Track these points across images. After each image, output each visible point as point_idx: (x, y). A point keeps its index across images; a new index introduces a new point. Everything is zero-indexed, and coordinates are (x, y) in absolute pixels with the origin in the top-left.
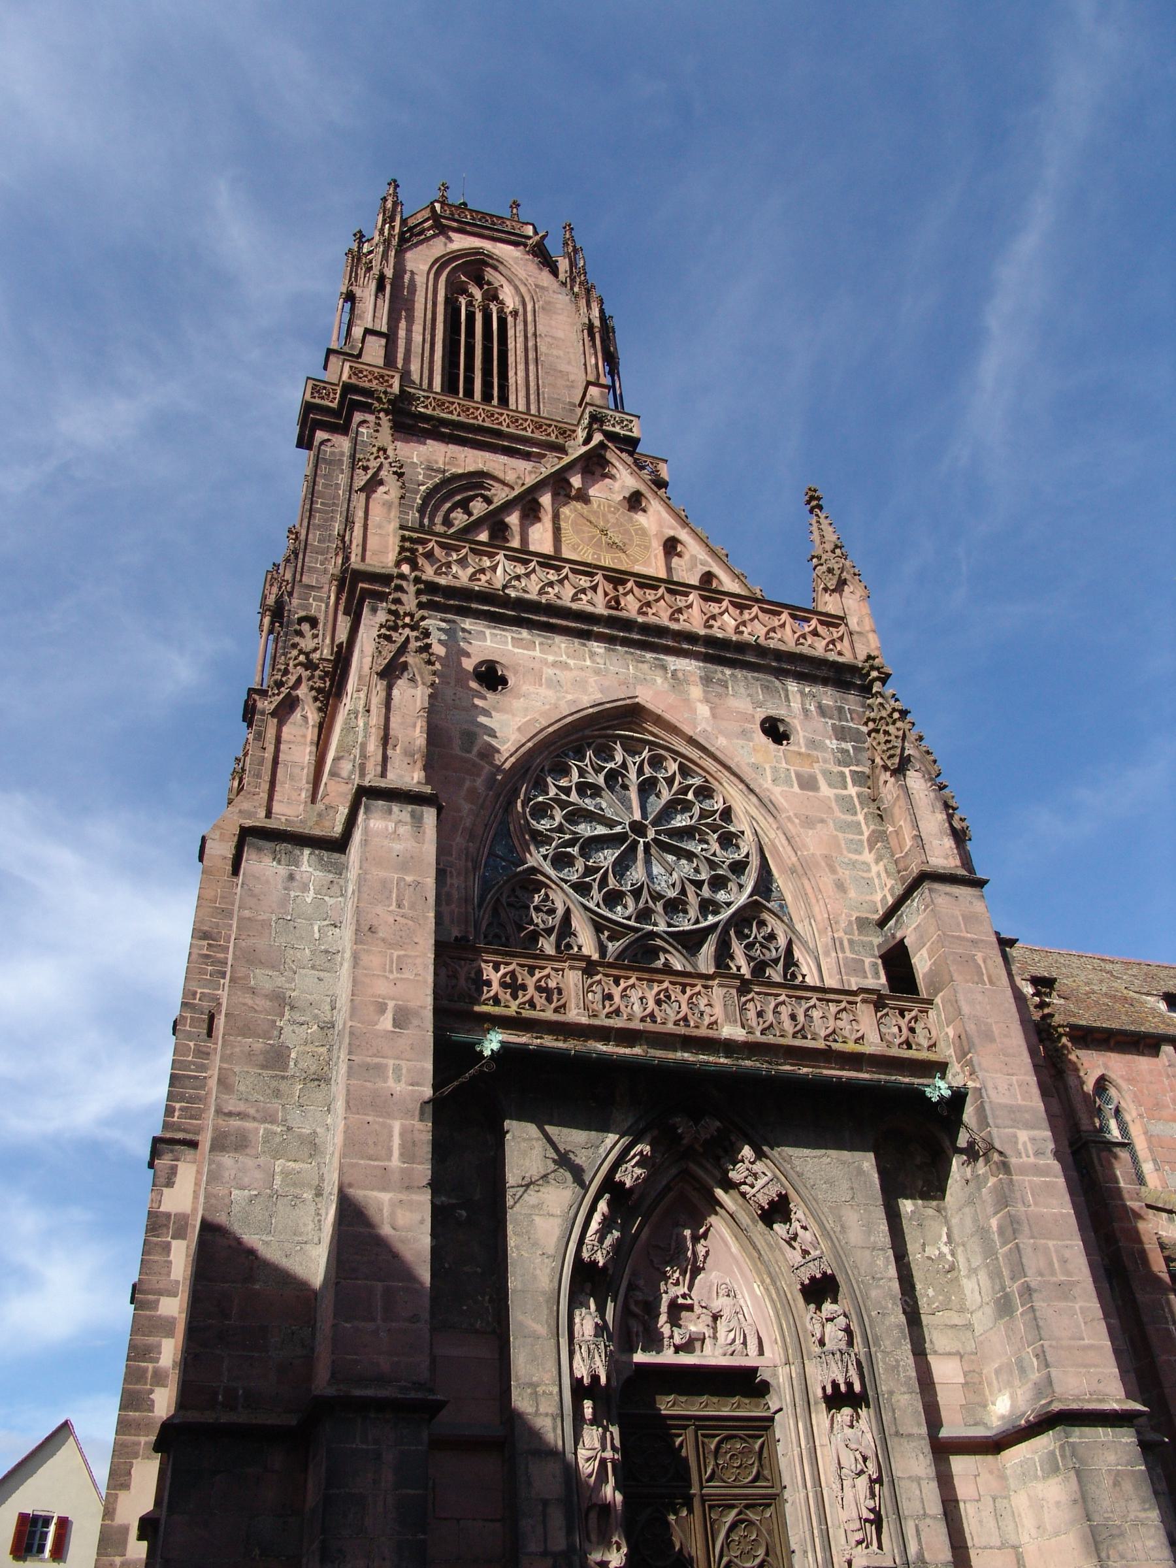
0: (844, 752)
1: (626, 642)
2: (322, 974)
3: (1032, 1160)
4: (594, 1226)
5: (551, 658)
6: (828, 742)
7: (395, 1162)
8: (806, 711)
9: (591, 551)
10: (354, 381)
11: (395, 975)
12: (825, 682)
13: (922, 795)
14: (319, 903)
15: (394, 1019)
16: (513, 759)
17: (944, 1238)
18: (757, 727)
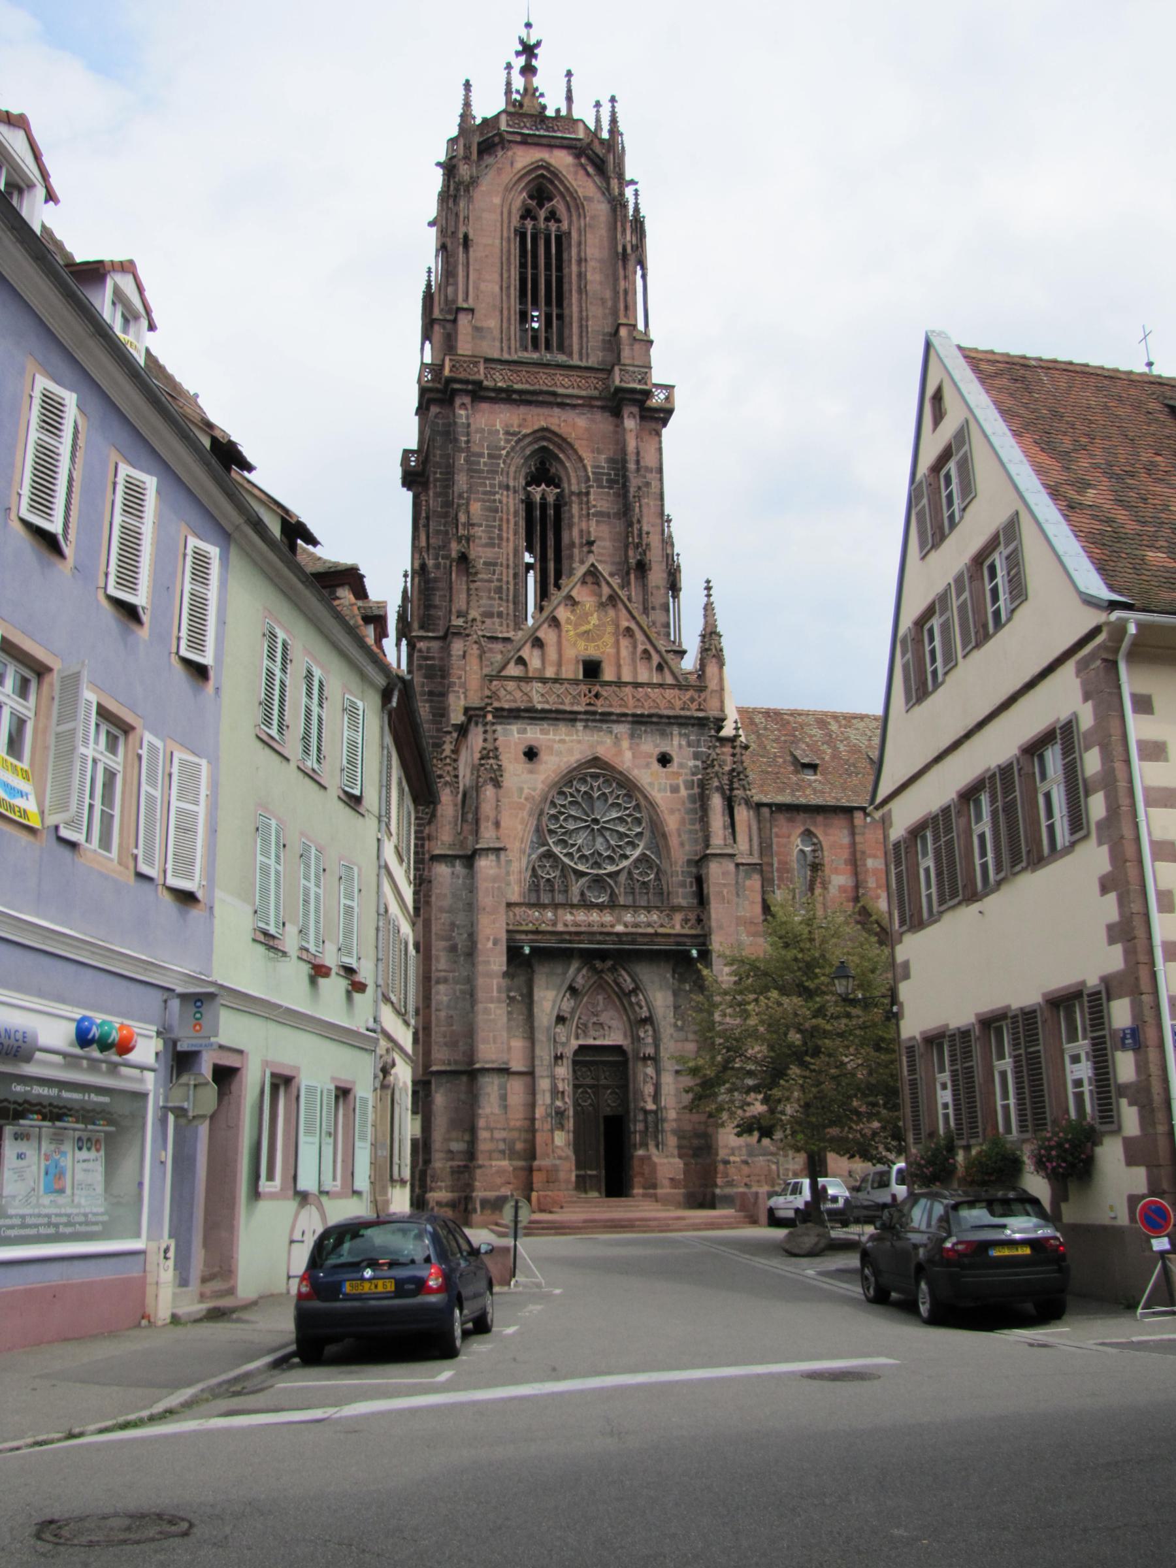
1: (594, 721)
5: (557, 738)
7: (495, 994)
8: (680, 746)
10: (453, 375)
12: (693, 725)
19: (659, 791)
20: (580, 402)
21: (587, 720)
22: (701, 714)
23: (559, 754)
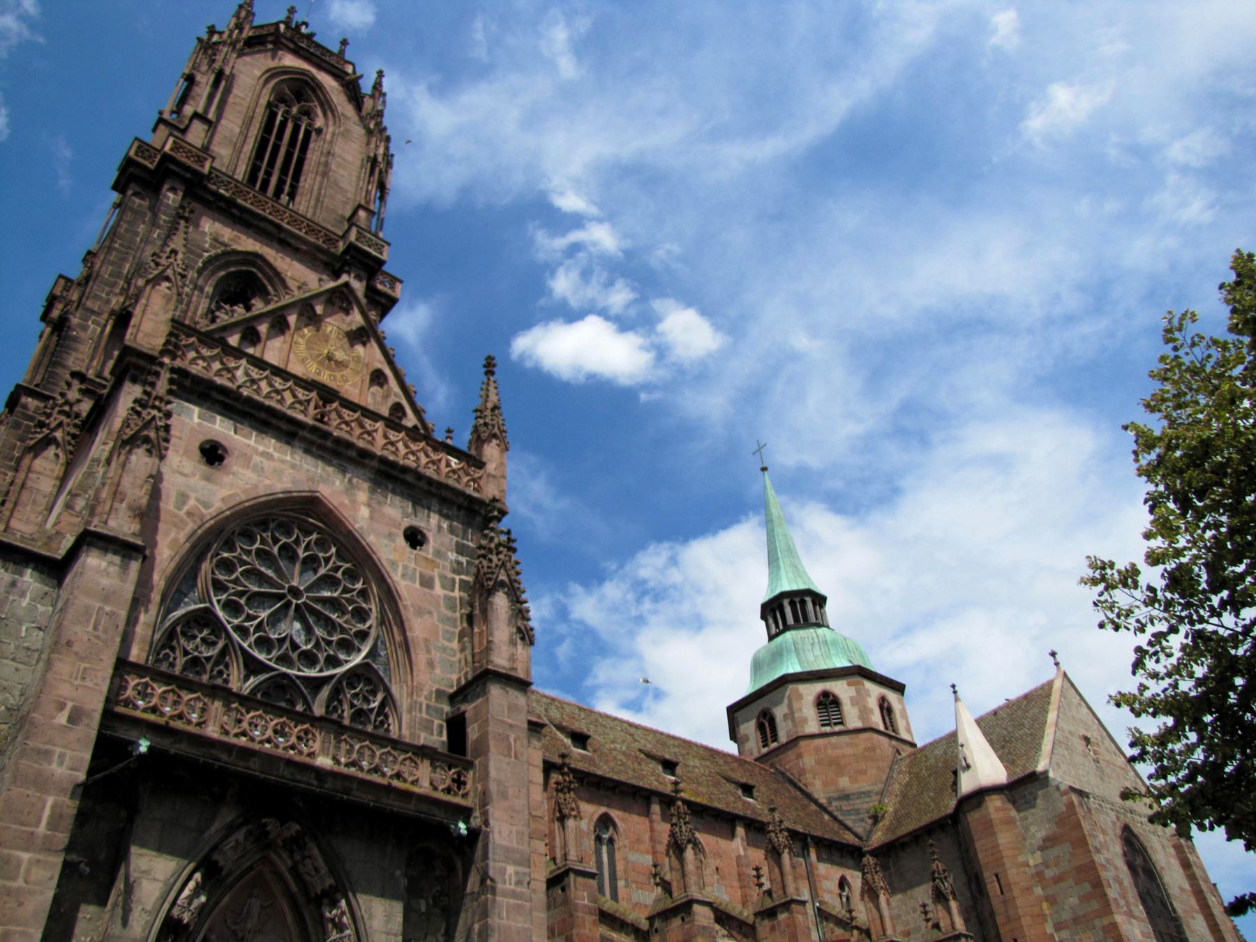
0: (459, 563)
1: (321, 447)
2: (20, 666)
3: (513, 887)
4: (186, 892)
6: (449, 554)
8: (440, 527)
9: (315, 366)
10: (172, 153)
11: (78, 682)
12: (460, 507)
13: (503, 611)
14: (31, 608)
15: (69, 717)
16: (212, 522)
17: (443, 931)
18: (401, 533)
19: (403, 576)
20: (304, 247)
21: (311, 443)
22: (475, 495)
23: (259, 470)
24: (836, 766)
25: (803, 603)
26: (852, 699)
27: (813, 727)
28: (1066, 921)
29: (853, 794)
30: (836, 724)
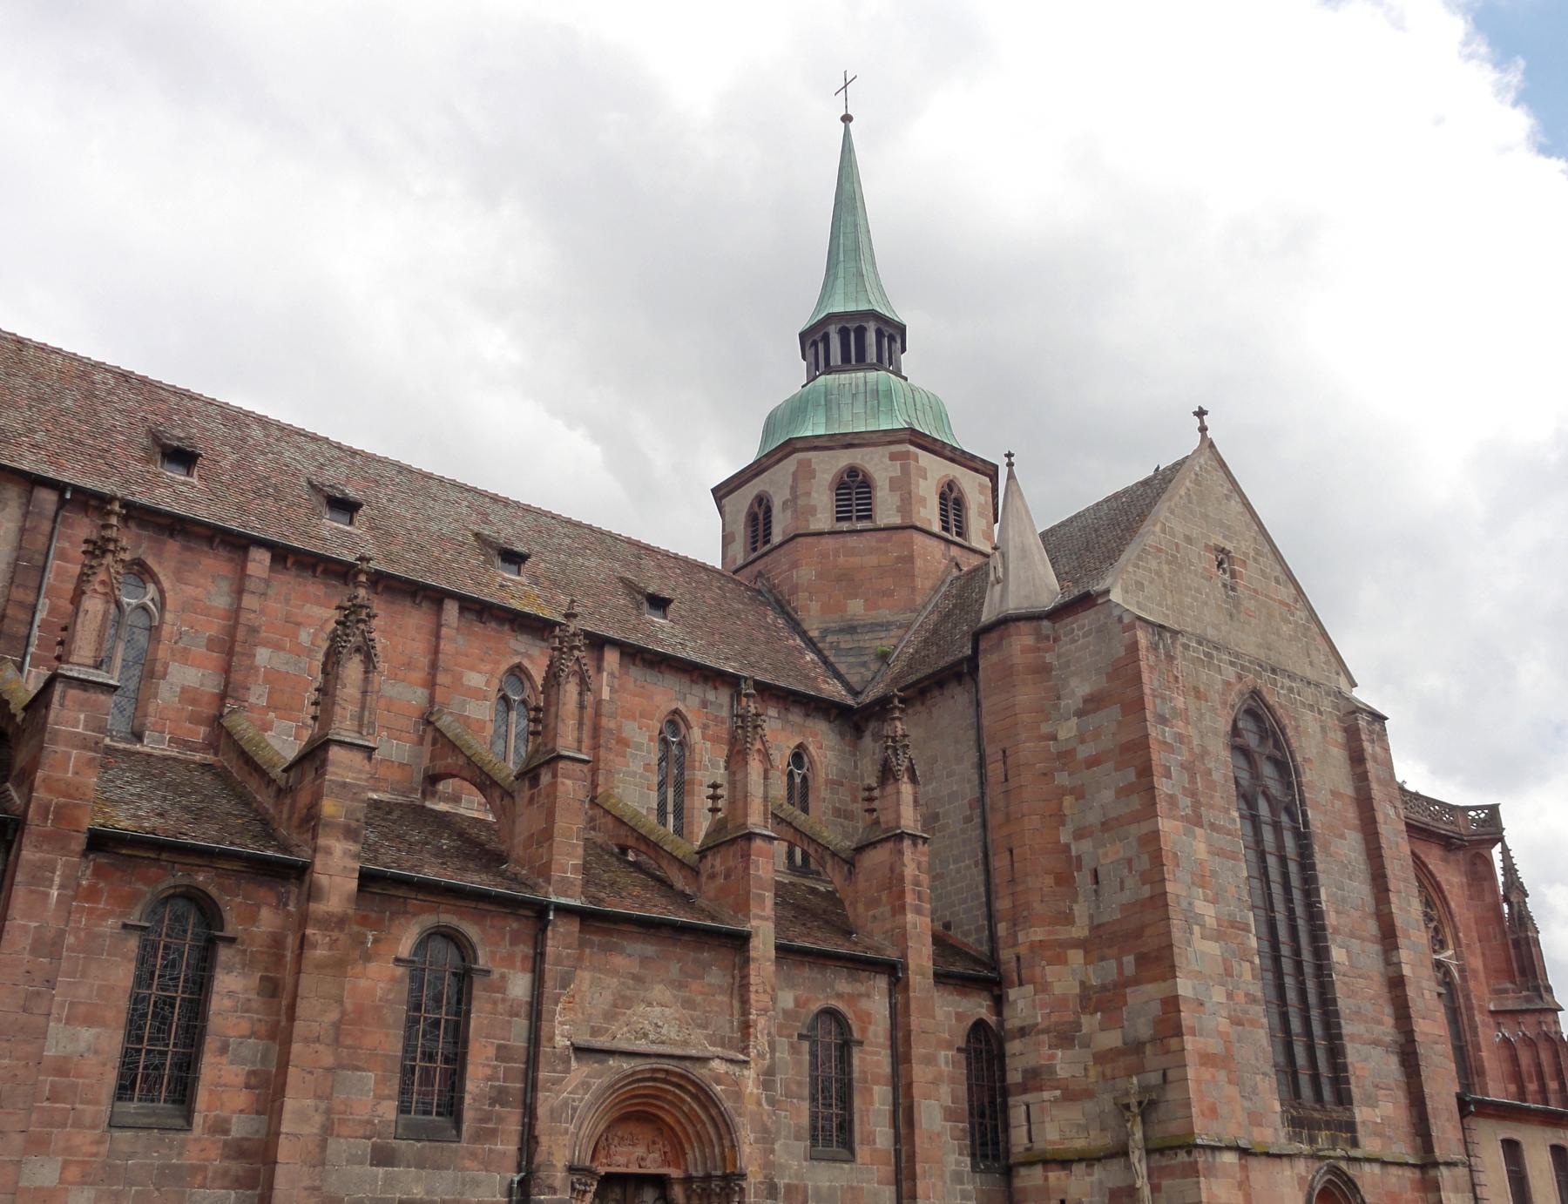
24: (848, 582)
25: (861, 332)
26: (892, 480)
27: (823, 519)
28: (1091, 825)
29: (864, 626)
30: (859, 518)
